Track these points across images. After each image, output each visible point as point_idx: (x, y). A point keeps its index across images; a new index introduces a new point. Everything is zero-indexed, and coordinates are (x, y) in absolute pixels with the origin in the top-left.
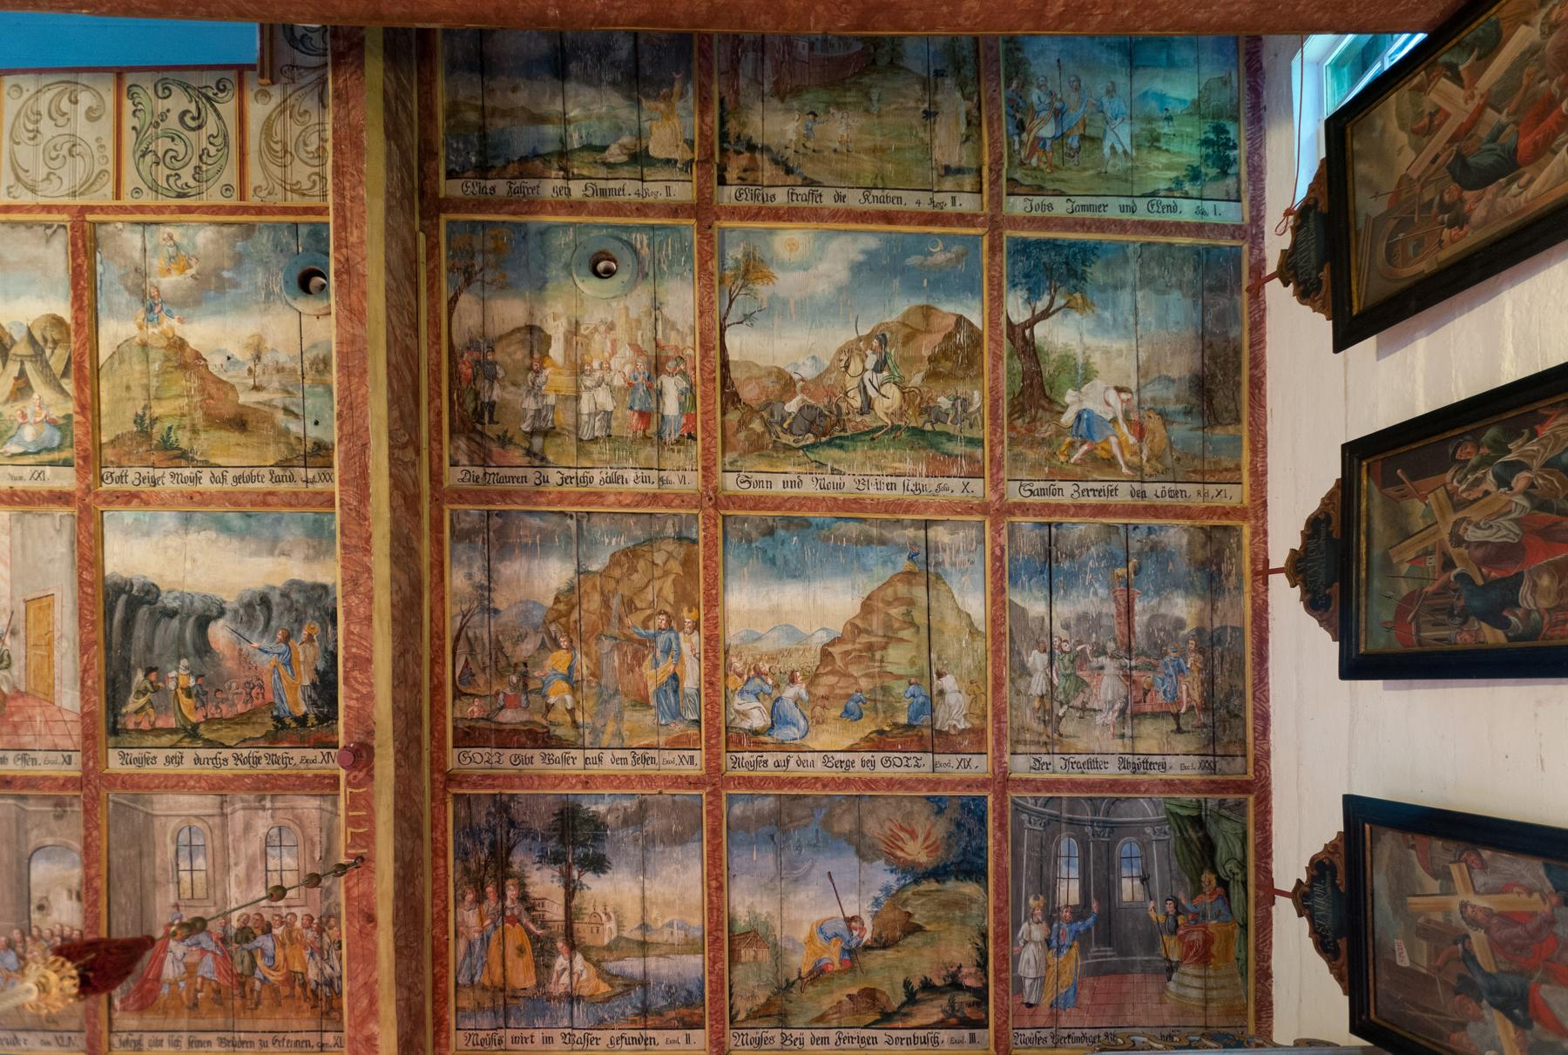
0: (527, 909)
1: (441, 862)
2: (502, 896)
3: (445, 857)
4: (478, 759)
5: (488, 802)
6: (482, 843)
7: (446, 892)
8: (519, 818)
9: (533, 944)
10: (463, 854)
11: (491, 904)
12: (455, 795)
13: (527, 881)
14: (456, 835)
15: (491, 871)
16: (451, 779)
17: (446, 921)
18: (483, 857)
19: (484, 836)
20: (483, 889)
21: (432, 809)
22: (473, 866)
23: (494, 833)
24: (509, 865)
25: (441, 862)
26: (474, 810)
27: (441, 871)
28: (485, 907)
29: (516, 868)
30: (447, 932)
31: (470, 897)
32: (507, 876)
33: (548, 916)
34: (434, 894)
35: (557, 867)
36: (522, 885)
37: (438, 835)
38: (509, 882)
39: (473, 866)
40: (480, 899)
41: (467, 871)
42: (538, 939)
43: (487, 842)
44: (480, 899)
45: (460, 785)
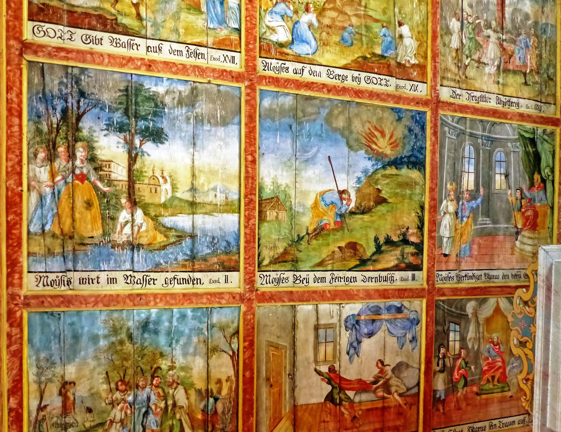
0: (95, 169)
1: (16, 121)
2: (72, 156)
3: (20, 116)
4: (52, 34)
5: (60, 73)
6: (54, 109)
7: (21, 149)
8: (88, 91)
9: (100, 199)
10: (36, 117)
11: (61, 163)
12: (29, 62)
13: (95, 145)
14: (30, 99)
15: (62, 133)
16: (26, 47)
17: (20, 174)
18: (55, 121)
19: (56, 102)
20: (54, 147)
21: (8, 72)
22: (45, 128)
23: (66, 102)
24: (78, 129)
25: (16, 121)
26: (47, 78)
27: (16, 129)
28: (56, 164)
29: (85, 133)
30: (21, 184)
31: (42, 155)
32: (76, 140)
33: (113, 176)
34: (8, 149)
35: (122, 135)
36: (90, 148)
37: (13, 96)
38: (79, 144)
39: (45, 128)
40: (51, 158)
41: (39, 131)
42: (104, 195)
43: (59, 108)
44: (51, 158)
45: (35, 53)
